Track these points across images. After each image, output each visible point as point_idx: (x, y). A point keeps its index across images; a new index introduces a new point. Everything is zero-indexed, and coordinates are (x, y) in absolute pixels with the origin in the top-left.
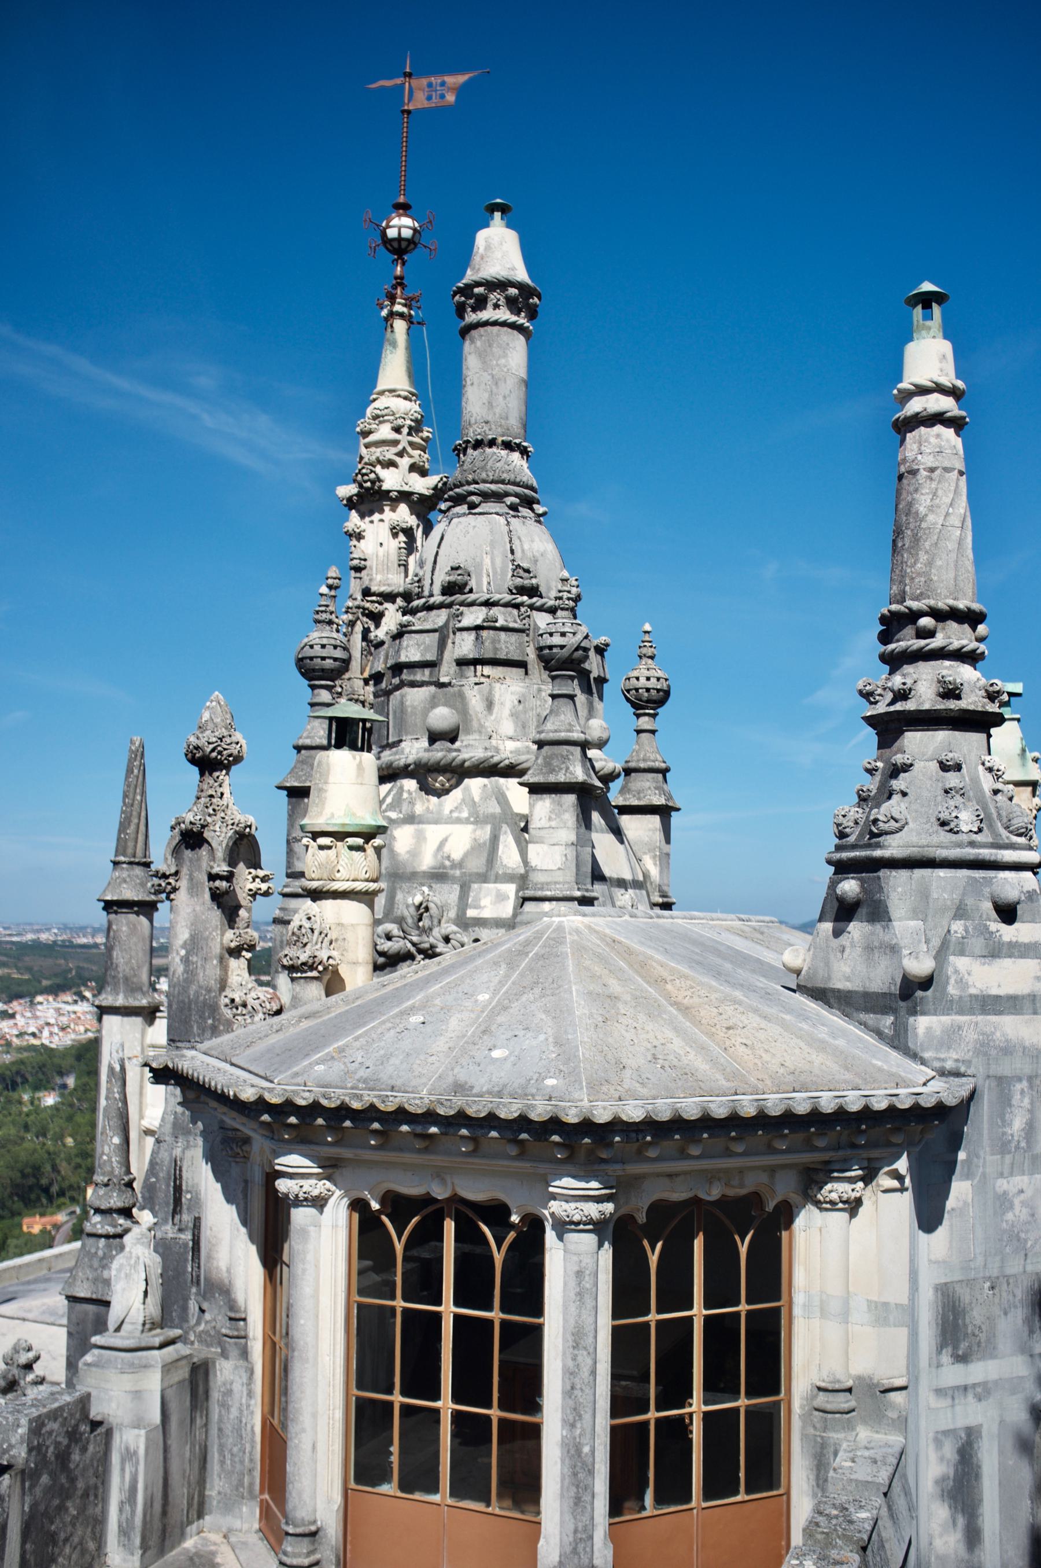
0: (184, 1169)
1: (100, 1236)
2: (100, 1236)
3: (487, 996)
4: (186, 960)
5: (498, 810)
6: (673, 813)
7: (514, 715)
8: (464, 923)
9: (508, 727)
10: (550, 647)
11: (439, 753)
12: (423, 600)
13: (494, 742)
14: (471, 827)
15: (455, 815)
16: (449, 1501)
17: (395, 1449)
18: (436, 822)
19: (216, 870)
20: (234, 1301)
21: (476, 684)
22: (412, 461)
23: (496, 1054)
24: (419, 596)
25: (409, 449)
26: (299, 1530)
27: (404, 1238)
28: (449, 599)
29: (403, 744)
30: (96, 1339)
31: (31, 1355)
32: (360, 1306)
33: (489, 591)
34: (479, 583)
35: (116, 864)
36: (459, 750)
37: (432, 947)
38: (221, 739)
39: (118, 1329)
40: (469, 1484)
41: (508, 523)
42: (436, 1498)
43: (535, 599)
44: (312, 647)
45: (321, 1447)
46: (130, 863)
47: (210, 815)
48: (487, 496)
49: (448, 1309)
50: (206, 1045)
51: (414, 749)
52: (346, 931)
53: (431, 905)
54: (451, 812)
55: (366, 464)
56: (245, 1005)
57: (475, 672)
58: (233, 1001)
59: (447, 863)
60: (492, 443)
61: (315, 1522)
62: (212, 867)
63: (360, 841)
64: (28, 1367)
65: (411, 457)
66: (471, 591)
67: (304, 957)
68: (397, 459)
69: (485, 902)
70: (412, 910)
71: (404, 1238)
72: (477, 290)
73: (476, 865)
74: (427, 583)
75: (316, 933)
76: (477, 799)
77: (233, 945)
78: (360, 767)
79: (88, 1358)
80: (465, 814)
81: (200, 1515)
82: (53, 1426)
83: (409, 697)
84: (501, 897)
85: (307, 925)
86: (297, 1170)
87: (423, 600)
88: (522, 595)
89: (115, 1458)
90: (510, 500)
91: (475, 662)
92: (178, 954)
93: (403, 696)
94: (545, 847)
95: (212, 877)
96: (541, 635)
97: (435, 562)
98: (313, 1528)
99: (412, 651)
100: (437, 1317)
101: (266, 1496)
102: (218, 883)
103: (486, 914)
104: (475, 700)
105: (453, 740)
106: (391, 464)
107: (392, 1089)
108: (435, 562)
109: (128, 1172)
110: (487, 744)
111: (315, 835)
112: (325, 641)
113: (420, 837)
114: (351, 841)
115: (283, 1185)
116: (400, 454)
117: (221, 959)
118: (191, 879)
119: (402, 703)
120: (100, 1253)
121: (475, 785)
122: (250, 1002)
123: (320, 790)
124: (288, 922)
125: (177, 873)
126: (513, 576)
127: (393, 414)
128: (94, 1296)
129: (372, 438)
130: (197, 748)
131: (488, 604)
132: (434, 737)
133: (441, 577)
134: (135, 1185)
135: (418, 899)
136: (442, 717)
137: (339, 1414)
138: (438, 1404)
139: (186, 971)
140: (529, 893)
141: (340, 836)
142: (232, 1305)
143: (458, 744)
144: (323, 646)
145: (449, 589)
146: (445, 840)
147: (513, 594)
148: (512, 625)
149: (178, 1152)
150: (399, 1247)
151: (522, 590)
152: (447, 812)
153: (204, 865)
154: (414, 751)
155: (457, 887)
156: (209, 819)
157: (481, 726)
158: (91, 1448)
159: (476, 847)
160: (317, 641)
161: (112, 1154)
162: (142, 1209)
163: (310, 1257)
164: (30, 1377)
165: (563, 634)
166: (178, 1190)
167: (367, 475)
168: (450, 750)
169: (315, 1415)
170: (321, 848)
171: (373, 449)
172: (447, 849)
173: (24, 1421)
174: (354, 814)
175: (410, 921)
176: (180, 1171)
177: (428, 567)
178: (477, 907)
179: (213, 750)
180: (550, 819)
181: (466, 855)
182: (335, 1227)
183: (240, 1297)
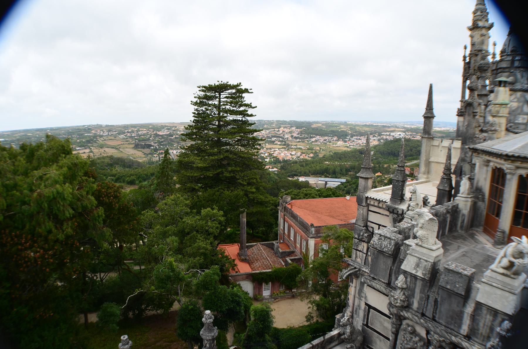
8: (516, 124)
64: (427, 200)
73: (519, 111)
74: (507, 49)
84: (524, 119)
89: (461, 215)
99: (504, 65)
103: (520, 122)
106: (480, 20)
121: (519, 94)
159: (518, 108)
166: (461, 172)
183: (484, 191)
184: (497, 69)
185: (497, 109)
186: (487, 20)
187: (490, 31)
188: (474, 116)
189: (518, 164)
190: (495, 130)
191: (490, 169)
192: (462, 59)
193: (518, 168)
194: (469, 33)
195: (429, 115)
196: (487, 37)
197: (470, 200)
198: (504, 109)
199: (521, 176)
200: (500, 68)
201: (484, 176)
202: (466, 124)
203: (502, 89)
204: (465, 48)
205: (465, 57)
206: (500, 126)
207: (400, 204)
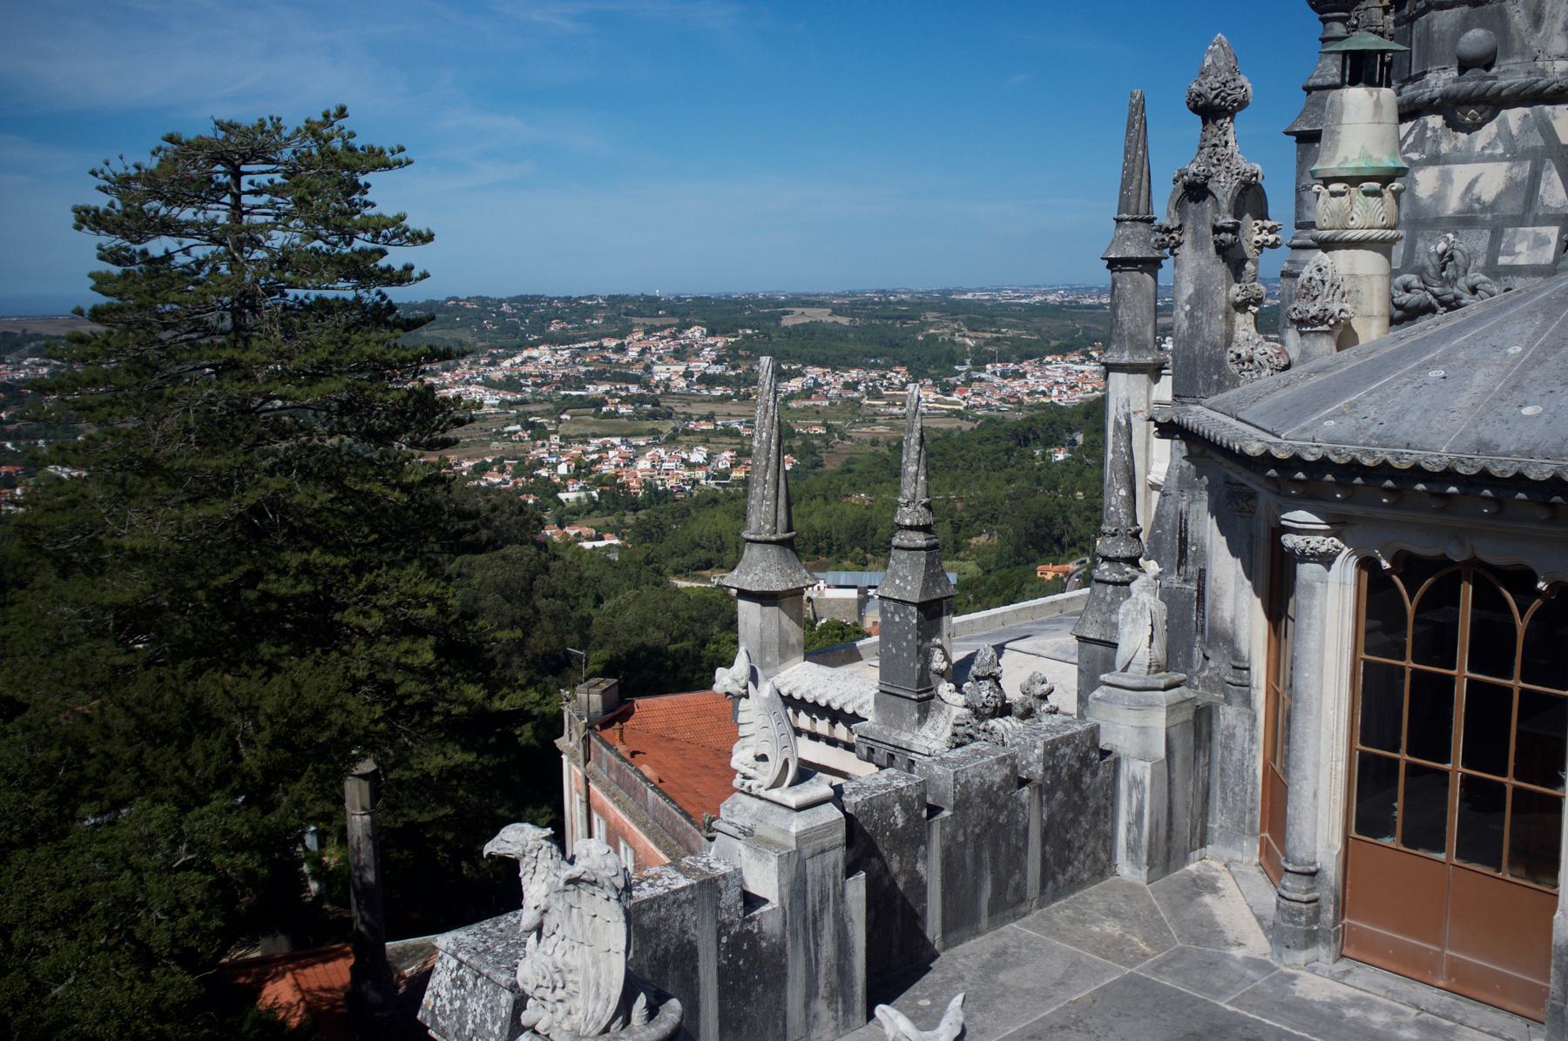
1: (1108, 583)
2: (1108, 583)
3: (1519, 349)
4: (1191, 316)
5: (1541, 143)
8: (1495, 272)
11: (1470, 83)
13: (1540, 64)
14: (1506, 165)
15: (1488, 152)
16: (1455, 861)
17: (1399, 805)
18: (1465, 161)
19: (1221, 222)
20: (1238, 651)
23: (1527, 411)
26: (1298, 869)
27: (1416, 599)
29: (1428, 76)
31: (1045, 687)
32: (1367, 663)
35: (1118, 221)
36: (1495, 78)
37: (1457, 298)
38: (1224, 84)
39: (1125, 669)
40: (1478, 847)
42: (1442, 856)
45: (1322, 795)
46: (1134, 220)
49: (1462, 673)
50: (1212, 400)
51: (1440, 80)
52: (1360, 281)
53: (1457, 253)
56: (1251, 361)
58: (1239, 356)
59: (1477, 206)
61: (1314, 863)
63: (1376, 185)
64: (1043, 698)
67: (1313, 311)
70: (1434, 259)
71: (1416, 599)
76: (1515, 132)
77: (1239, 299)
78: (1378, 105)
79: (1097, 693)
81: (1203, 844)
82: (1064, 750)
83: (1436, 22)
84: (1541, 242)
85: (1318, 277)
86: (1303, 525)
89: (1123, 785)
93: (1429, 21)
95: (1217, 230)
98: (1312, 869)
100: (1450, 680)
101: (1267, 835)
102: (1223, 236)
103: (1522, 260)
105: (1488, 67)
107: (1408, 446)
109: (1135, 523)
110: (1531, 68)
111: (1327, 182)
113: (1446, 180)
114: (1366, 185)
115: (1289, 540)
117: (1227, 314)
118: (1195, 232)
119: (1428, 29)
120: (1108, 598)
122: (1257, 357)
123: (1333, 133)
124: (1297, 275)
125: (1180, 227)
130: (1199, 95)
132: (1464, 65)
134: (1141, 536)
135: (1442, 246)
136: (1475, 39)
137: (1342, 766)
138: (1449, 766)
139: (1190, 327)
141: (1353, 181)
142: (1236, 654)
143: (1494, 70)
146: (1475, 181)
149: (1183, 505)
150: (1410, 608)
152: (1478, 148)
153: (1209, 218)
154: (1440, 83)
155: (1487, 233)
156: (1213, 170)
157: (1525, 46)
158: (1101, 773)
159: (1512, 187)
162: (1148, 559)
163: (1315, 612)
164: (1045, 707)
166: (1183, 542)
168: (1485, 79)
169: (1317, 765)
170: (1333, 194)
172: (1476, 190)
173: (1040, 744)
174: (1370, 157)
175: (1431, 271)
178: (1512, 253)
179: (1216, 96)
181: (1499, 196)
182: (1342, 584)
183: (1244, 648)
203: (1357, 98)
207: (921, 721)
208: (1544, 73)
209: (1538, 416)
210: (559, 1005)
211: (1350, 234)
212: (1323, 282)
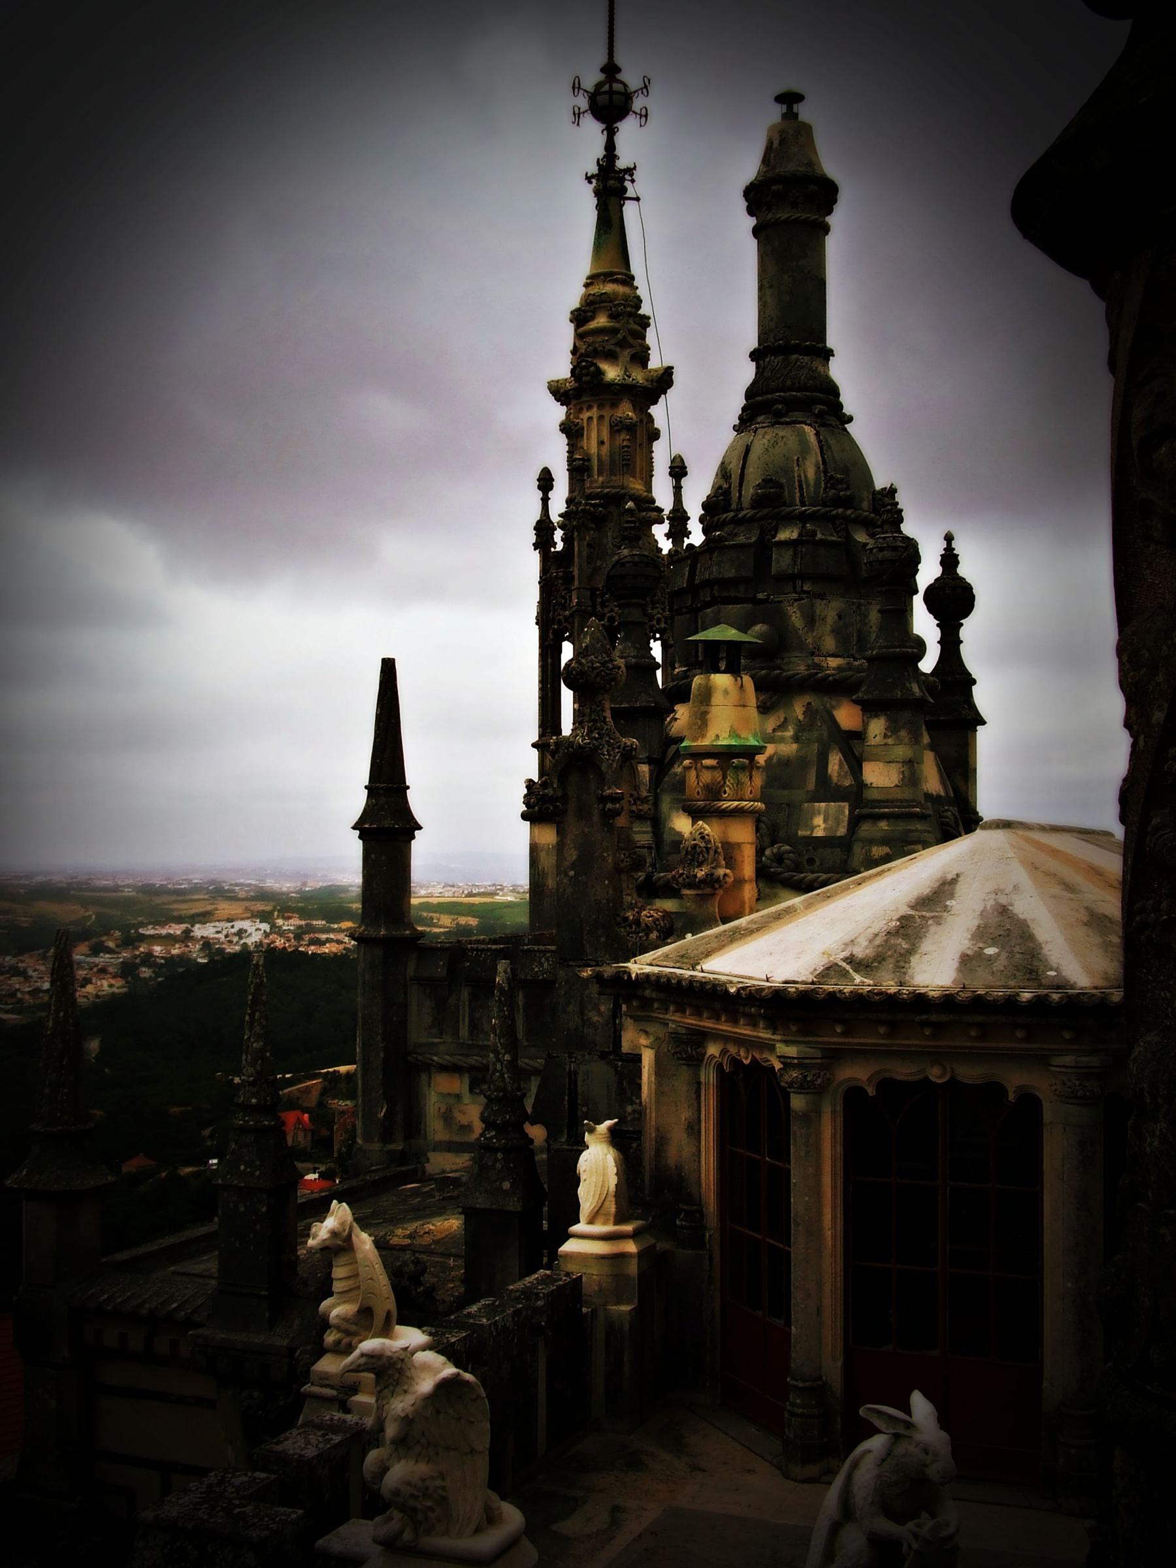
0: (579, 1083)
2: (498, 1150)
6: (978, 728)
7: (836, 632)
9: (829, 643)
10: (881, 562)
12: (732, 514)
21: (796, 600)
22: (633, 351)
24: (727, 509)
25: (631, 340)
28: (765, 511)
30: (575, 1229)
33: (803, 504)
34: (792, 497)
38: (603, 664)
41: (817, 434)
43: (849, 512)
44: (623, 565)
47: (596, 739)
48: (793, 405)
54: (774, 730)
55: (582, 355)
57: (795, 588)
60: (798, 349)
62: (603, 791)
65: (632, 346)
66: (784, 504)
67: (701, 873)
68: (618, 349)
69: (819, 821)
72: (774, 188)
74: (735, 495)
75: (712, 852)
79: (570, 1246)
80: (790, 733)
87: (732, 514)
88: (837, 507)
90: (818, 408)
91: (792, 578)
92: (566, 875)
94: (881, 765)
95: (603, 800)
96: (871, 549)
97: (742, 475)
102: (609, 806)
103: (819, 833)
104: (796, 619)
106: (611, 357)
108: (742, 475)
112: (636, 559)
116: (623, 344)
120: (498, 1166)
126: (826, 487)
127: (611, 301)
128: (494, 1207)
129: (593, 325)
131: (803, 518)
133: (749, 491)
140: (865, 811)
143: (778, 661)
144: (635, 564)
145: (757, 502)
147: (826, 506)
148: (830, 538)
151: (837, 502)
152: (770, 730)
160: (629, 559)
161: (505, 1070)
165: (895, 549)
167: (584, 367)
171: (590, 339)
174: (738, 736)
176: (576, 1086)
177: (735, 479)
179: (597, 676)
180: (885, 736)
182: (834, 1112)
184: (693, 589)
185: (707, 777)
186: (641, 357)
187: (654, 410)
188: (608, 816)
189: (835, 1037)
190: (712, 882)
191: (709, 1076)
192: (532, 537)
193: (834, 1056)
194: (559, 412)
195: (388, 823)
196: (641, 433)
197: (631, 1247)
198: (744, 778)
199: (854, 1094)
200: (709, 583)
201: (685, 1115)
202: (572, 855)
204: (546, 482)
205: (543, 529)
206: (731, 862)
208: (818, 667)
209: (998, 955)
210: (430, 1514)
211: (725, 805)
212: (708, 849)
